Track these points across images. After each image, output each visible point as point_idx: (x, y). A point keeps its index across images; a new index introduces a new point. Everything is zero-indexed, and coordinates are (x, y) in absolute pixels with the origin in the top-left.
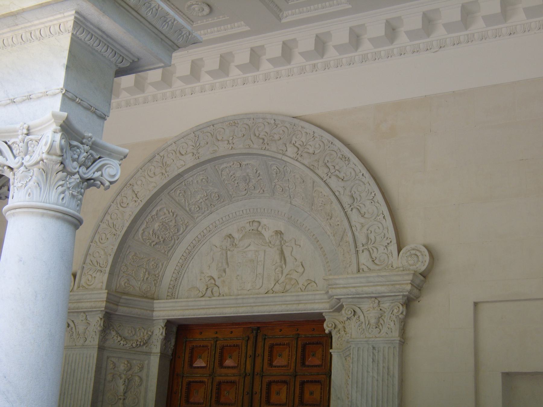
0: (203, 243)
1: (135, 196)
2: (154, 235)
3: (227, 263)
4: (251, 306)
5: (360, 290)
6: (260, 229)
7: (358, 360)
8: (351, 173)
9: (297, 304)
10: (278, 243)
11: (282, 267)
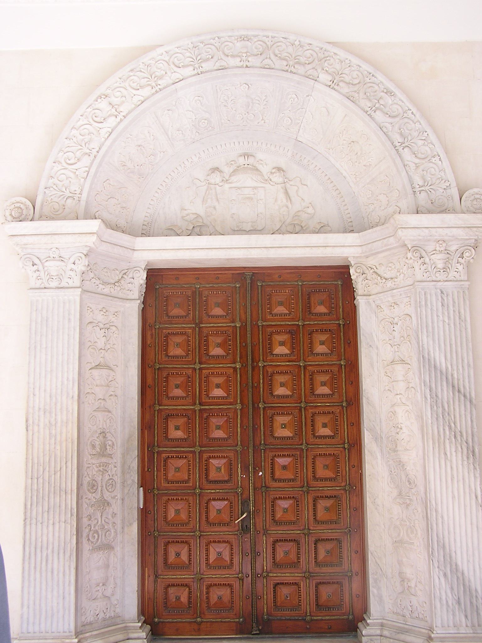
1: (114, 110)
2: (130, 161)
3: (217, 200)
7: (426, 305)
8: (397, 109)
11: (287, 207)
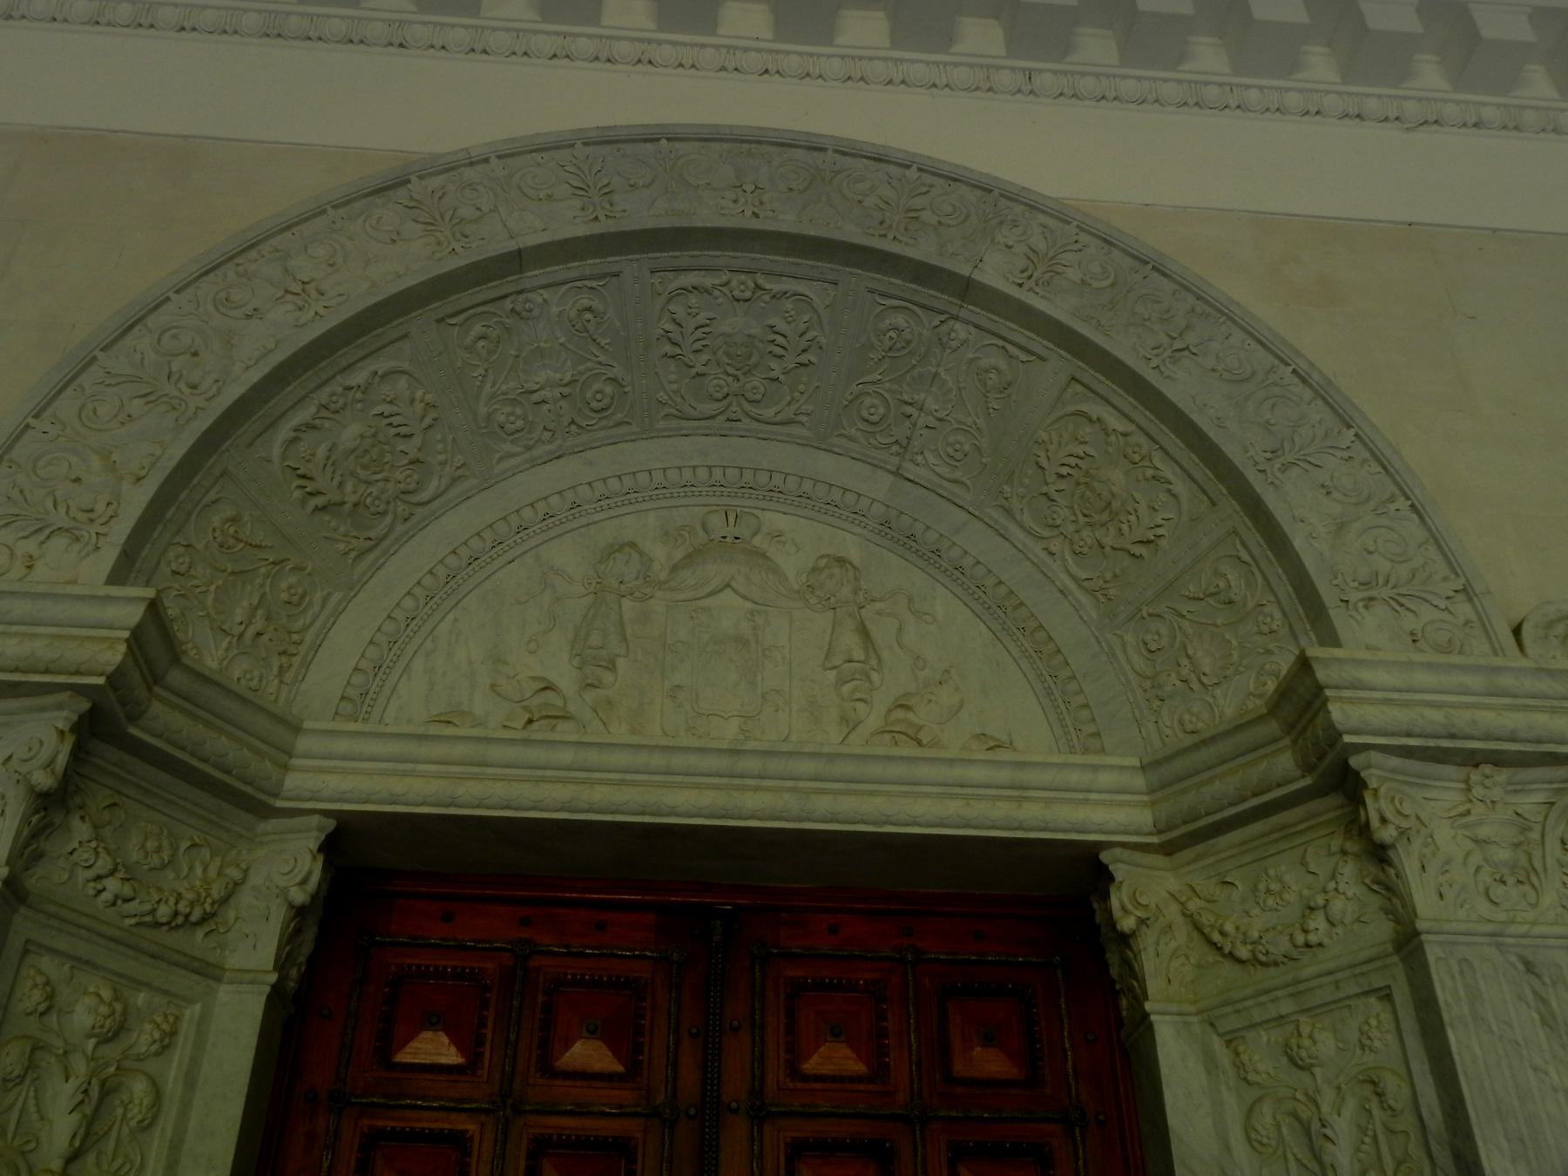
0: (509, 556)
2: (329, 469)
3: (624, 639)
4: (794, 790)
5: (1462, 719)
9: (1009, 798)
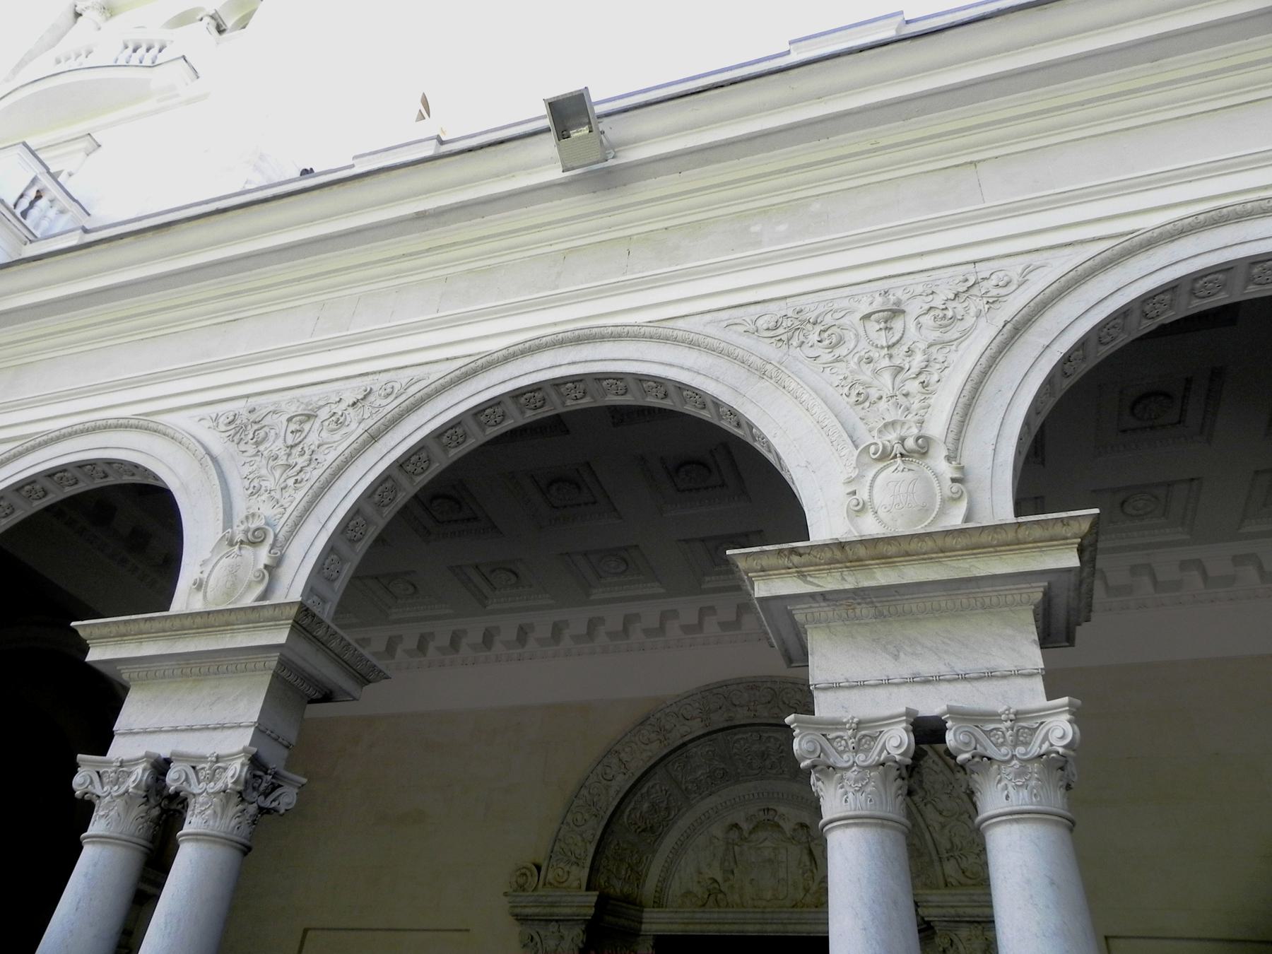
5: (961, 911)
6: (776, 819)
10: (804, 839)
